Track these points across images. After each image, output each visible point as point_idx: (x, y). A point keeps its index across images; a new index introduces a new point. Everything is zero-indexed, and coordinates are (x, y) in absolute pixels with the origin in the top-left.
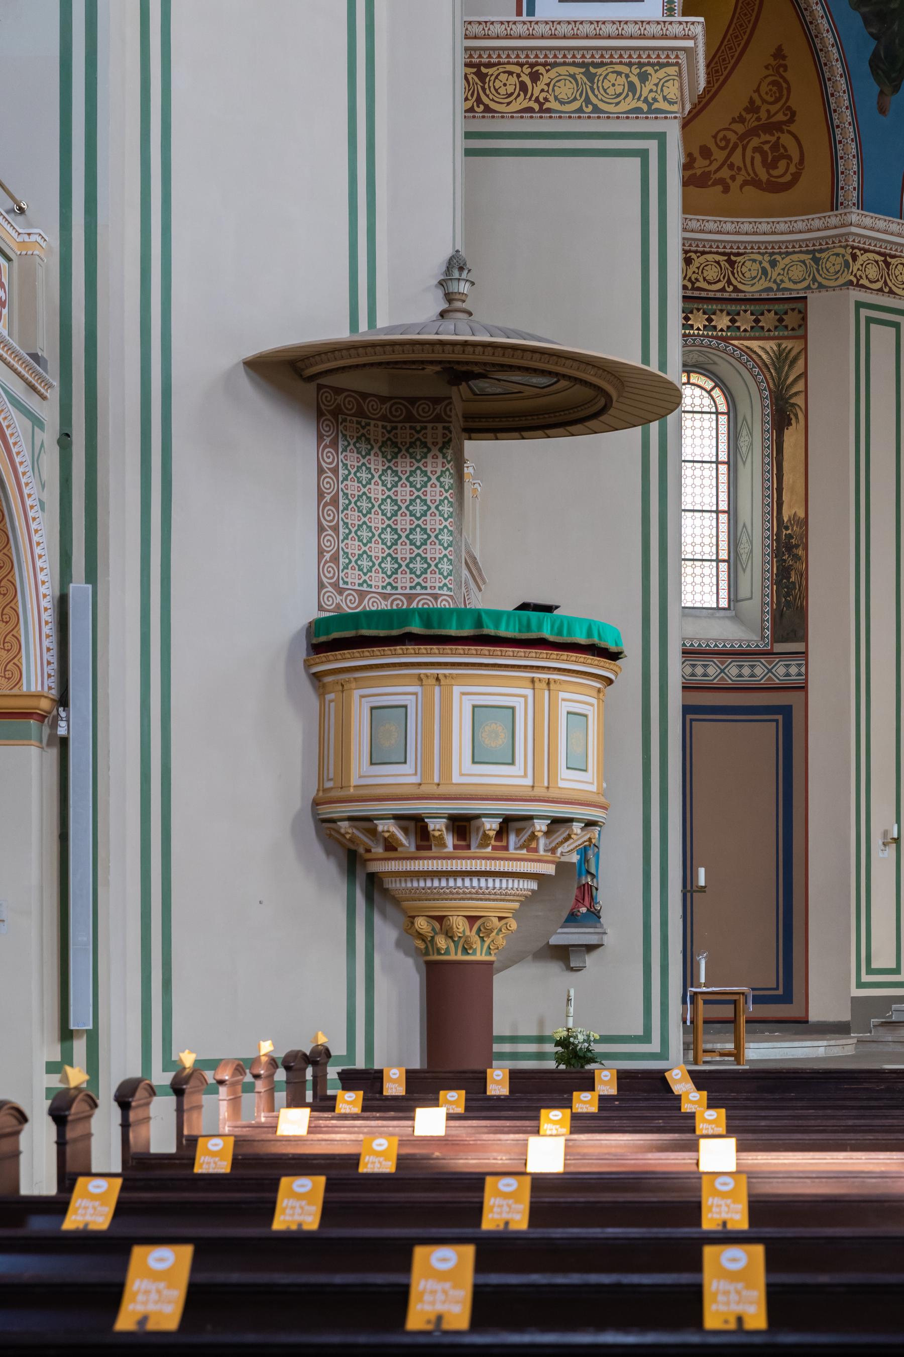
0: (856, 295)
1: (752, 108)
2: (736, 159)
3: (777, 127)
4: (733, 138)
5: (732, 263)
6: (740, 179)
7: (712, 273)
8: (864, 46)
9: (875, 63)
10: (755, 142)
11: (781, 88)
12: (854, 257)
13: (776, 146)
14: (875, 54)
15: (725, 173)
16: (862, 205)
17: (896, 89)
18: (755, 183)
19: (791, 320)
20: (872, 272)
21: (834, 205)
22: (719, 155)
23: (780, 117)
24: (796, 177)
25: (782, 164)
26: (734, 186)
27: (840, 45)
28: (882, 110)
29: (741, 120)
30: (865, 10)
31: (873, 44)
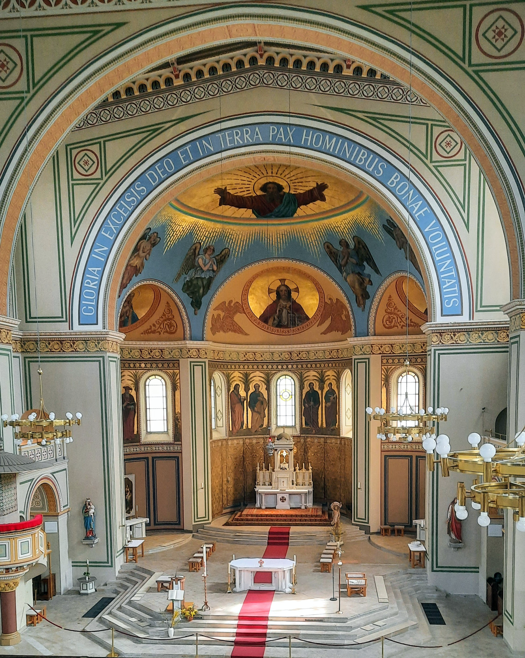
1: (164, 315)
2: (162, 326)
3: (171, 319)
4: (160, 322)
5: (162, 351)
6: (163, 331)
7: (157, 354)
8: (188, 300)
9: (192, 304)
10: (166, 322)
11: (170, 311)
12: (189, 351)
13: (171, 323)
14: (192, 301)
15: (159, 330)
17: (199, 308)
18: (167, 332)
19: (176, 365)
20: (195, 354)
21: (184, 340)
22: (157, 326)
23: (171, 317)
24: (176, 330)
25: (173, 327)
26: (162, 333)
27: (181, 301)
28: (195, 314)
29: (162, 317)
30: (188, 292)
31: (191, 299)
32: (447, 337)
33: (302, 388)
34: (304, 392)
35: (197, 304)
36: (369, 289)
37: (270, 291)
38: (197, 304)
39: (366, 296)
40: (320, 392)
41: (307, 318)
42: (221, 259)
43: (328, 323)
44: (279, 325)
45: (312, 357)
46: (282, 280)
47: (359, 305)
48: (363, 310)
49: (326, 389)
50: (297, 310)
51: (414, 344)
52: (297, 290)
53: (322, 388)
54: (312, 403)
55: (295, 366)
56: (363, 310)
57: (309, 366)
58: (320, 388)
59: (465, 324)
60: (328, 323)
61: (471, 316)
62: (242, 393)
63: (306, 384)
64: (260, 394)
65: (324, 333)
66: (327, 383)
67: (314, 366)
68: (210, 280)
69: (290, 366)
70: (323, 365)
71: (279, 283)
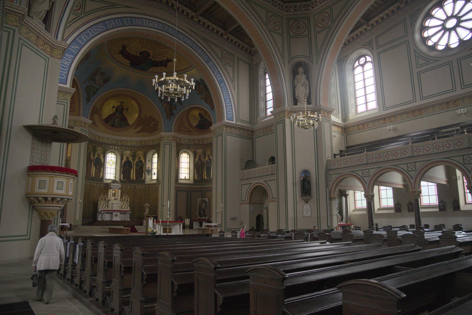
0: (81, 128)
16: (83, 116)
32: (229, 129)
33: (122, 159)
34: (123, 161)
35: (88, 100)
36: (174, 111)
37: (114, 107)
38: (88, 100)
39: (172, 114)
40: (132, 162)
41: (128, 125)
42: (106, 81)
43: (139, 129)
44: (113, 126)
45: (129, 144)
46: (122, 103)
47: (168, 118)
48: (170, 121)
49: (137, 160)
50: (124, 120)
51: (189, 140)
52: (127, 109)
53: (134, 160)
54: (128, 167)
55: (119, 148)
56: (170, 121)
57: (127, 148)
58: (132, 160)
59: (234, 124)
60: (139, 129)
61: (236, 122)
62: (92, 157)
63: (125, 157)
64: (101, 160)
65: (137, 133)
66: (137, 157)
67: (130, 148)
68: (98, 89)
69: (116, 147)
70: (135, 148)
71: (119, 104)
